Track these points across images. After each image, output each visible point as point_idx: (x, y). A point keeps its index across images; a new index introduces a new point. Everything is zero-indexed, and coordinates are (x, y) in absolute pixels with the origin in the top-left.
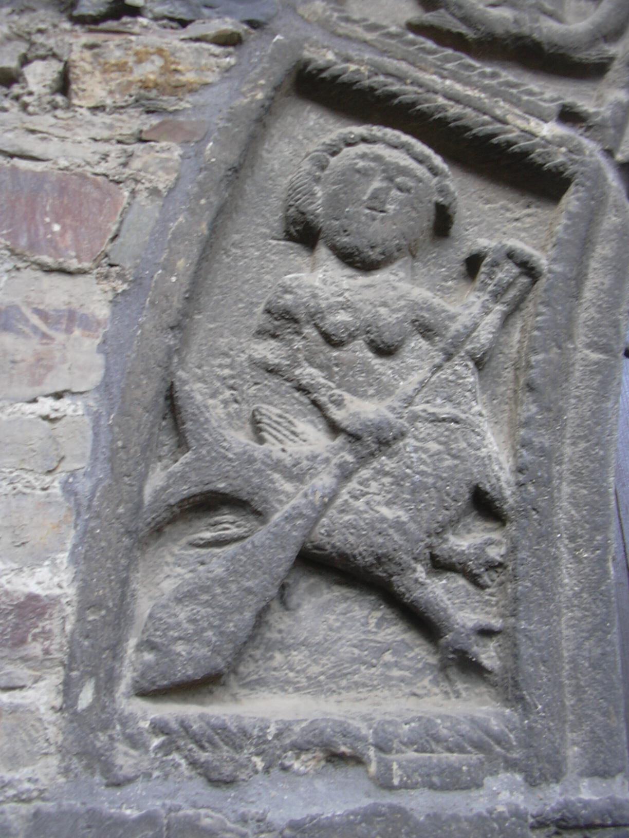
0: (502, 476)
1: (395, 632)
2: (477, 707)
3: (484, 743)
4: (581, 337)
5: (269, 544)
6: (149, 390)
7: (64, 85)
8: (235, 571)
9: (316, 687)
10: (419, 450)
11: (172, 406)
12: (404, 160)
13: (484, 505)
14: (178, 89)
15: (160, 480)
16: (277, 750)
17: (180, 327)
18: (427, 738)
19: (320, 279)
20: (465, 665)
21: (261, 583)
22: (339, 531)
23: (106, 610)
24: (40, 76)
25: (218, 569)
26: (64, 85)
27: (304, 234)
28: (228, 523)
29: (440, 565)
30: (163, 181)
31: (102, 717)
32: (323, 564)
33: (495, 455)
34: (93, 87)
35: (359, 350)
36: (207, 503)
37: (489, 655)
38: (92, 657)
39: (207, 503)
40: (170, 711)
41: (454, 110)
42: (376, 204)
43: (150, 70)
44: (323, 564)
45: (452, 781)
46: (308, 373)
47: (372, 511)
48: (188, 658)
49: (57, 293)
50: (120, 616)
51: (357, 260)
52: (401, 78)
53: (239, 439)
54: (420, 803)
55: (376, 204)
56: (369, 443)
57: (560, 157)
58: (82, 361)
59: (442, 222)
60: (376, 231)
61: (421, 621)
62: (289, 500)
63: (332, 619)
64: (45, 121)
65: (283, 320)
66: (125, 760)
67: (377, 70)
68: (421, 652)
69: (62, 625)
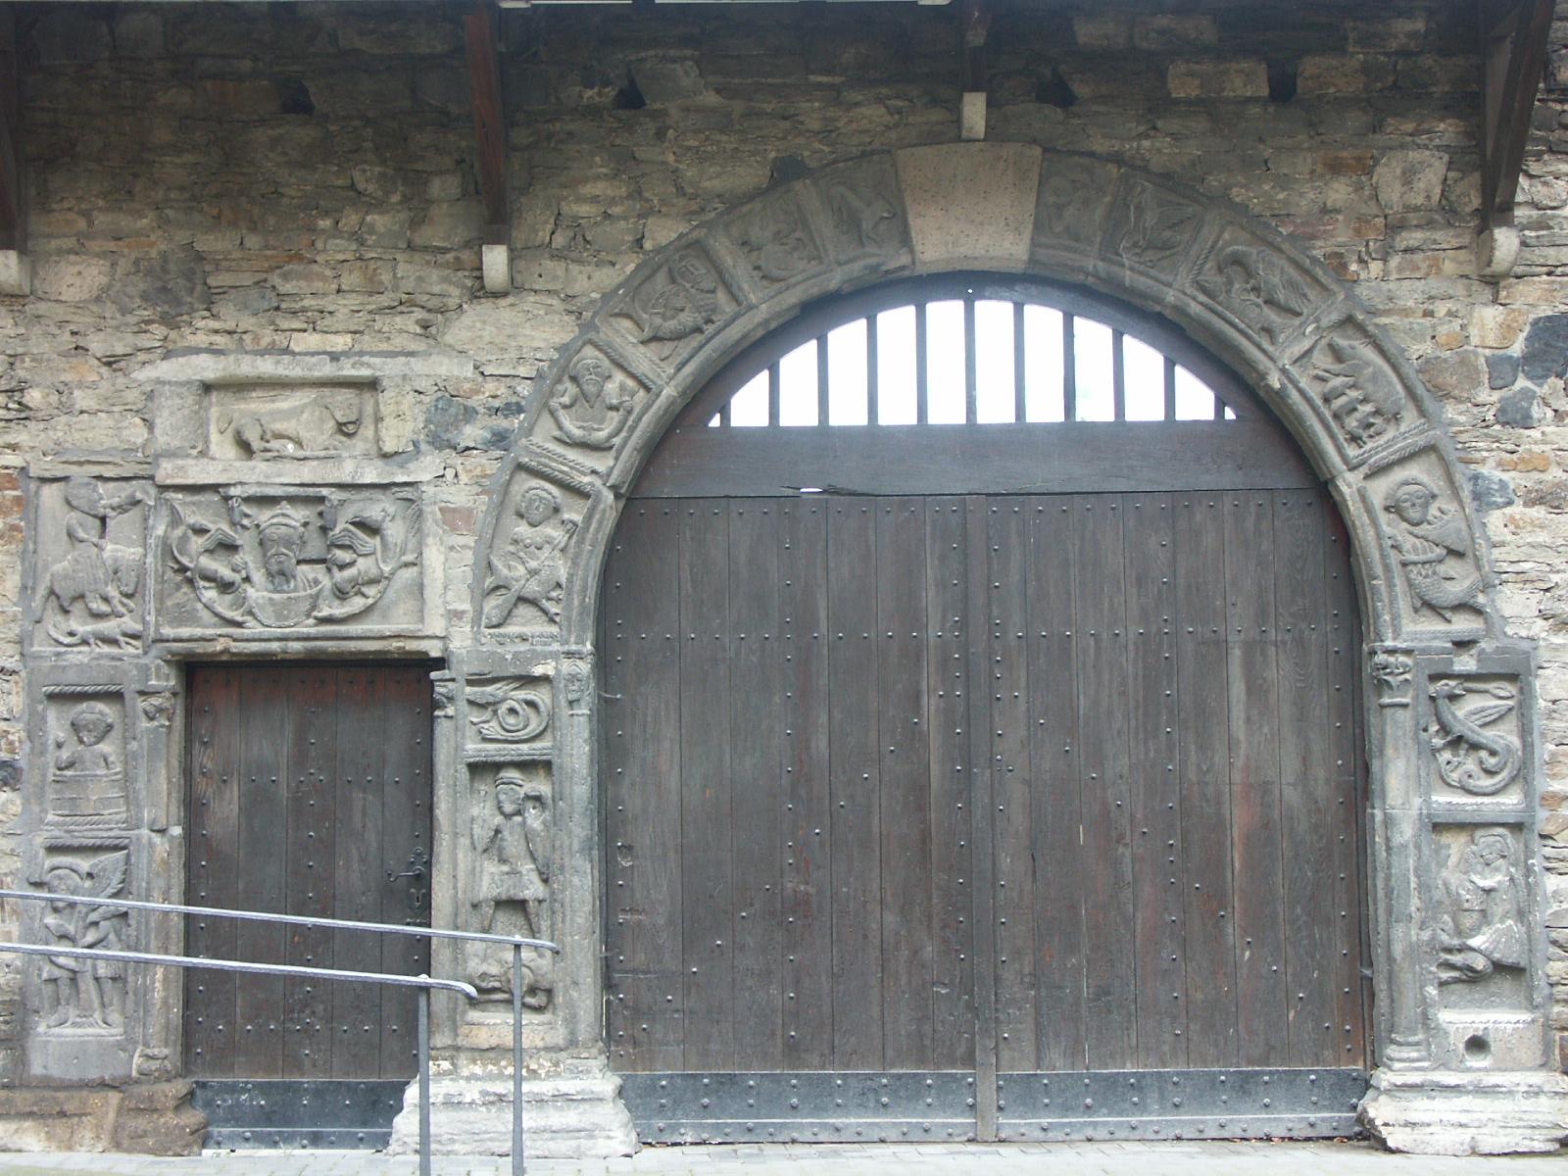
0: (563, 581)
1: (540, 613)
2: (554, 629)
3: (552, 637)
4: (588, 542)
5: (511, 596)
6: (484, 564)
7: (456, 476)
8: (505, 601)
9: (523, 625)
10: (544, 574)
11: (490, 565)
12: (544, 494)
13: (559, 585)
14: (485, 476)
15: (489, 582)
16: (512, 638)
17: (491, 547)
18: (541, 636)
19: (523, 529)
20: (552, 621)
21: (509, 606)
22: (525, 593)
23: (479, 612)
24: (450, 473)
25: (500, 602)
26: (456, 476)
27: (521, 516)
28: (503, 591)
29: (549, 599)
30: (484, 508)
31: (479, 632)
32: (522, 599)
33: (563, 575)
34: (464, 478)
35: (532, 548)
36: (498, 588)
37: (557, 619)
38: (476, 622)
39: (498, 588)
40: (492, 631)
41: (561, 476)
42: (537, 508)
43: (478, 471)
44: (522, 599)
45: (545, 644)
46: (522, 554)
47: (533, 588)
48: (495, 621)
49: (460, 540)
50: (481, 612)
51: (532, 525)
52: (546, 466)
53: (505, 571)
54: (539, 648)
55: (537, 508)
56: (533, 573)
57: (588, 488)
58: (469, 557)
59: (557, 510)
60: (536, 516)
61: (545, 612)
62: (516, 586)
63: (524, 610)
64: (453, 489)
65: (516, 542)
66: (483, 640)
67: (539, 463)
68: (544, 618)
69: (470, 615)
